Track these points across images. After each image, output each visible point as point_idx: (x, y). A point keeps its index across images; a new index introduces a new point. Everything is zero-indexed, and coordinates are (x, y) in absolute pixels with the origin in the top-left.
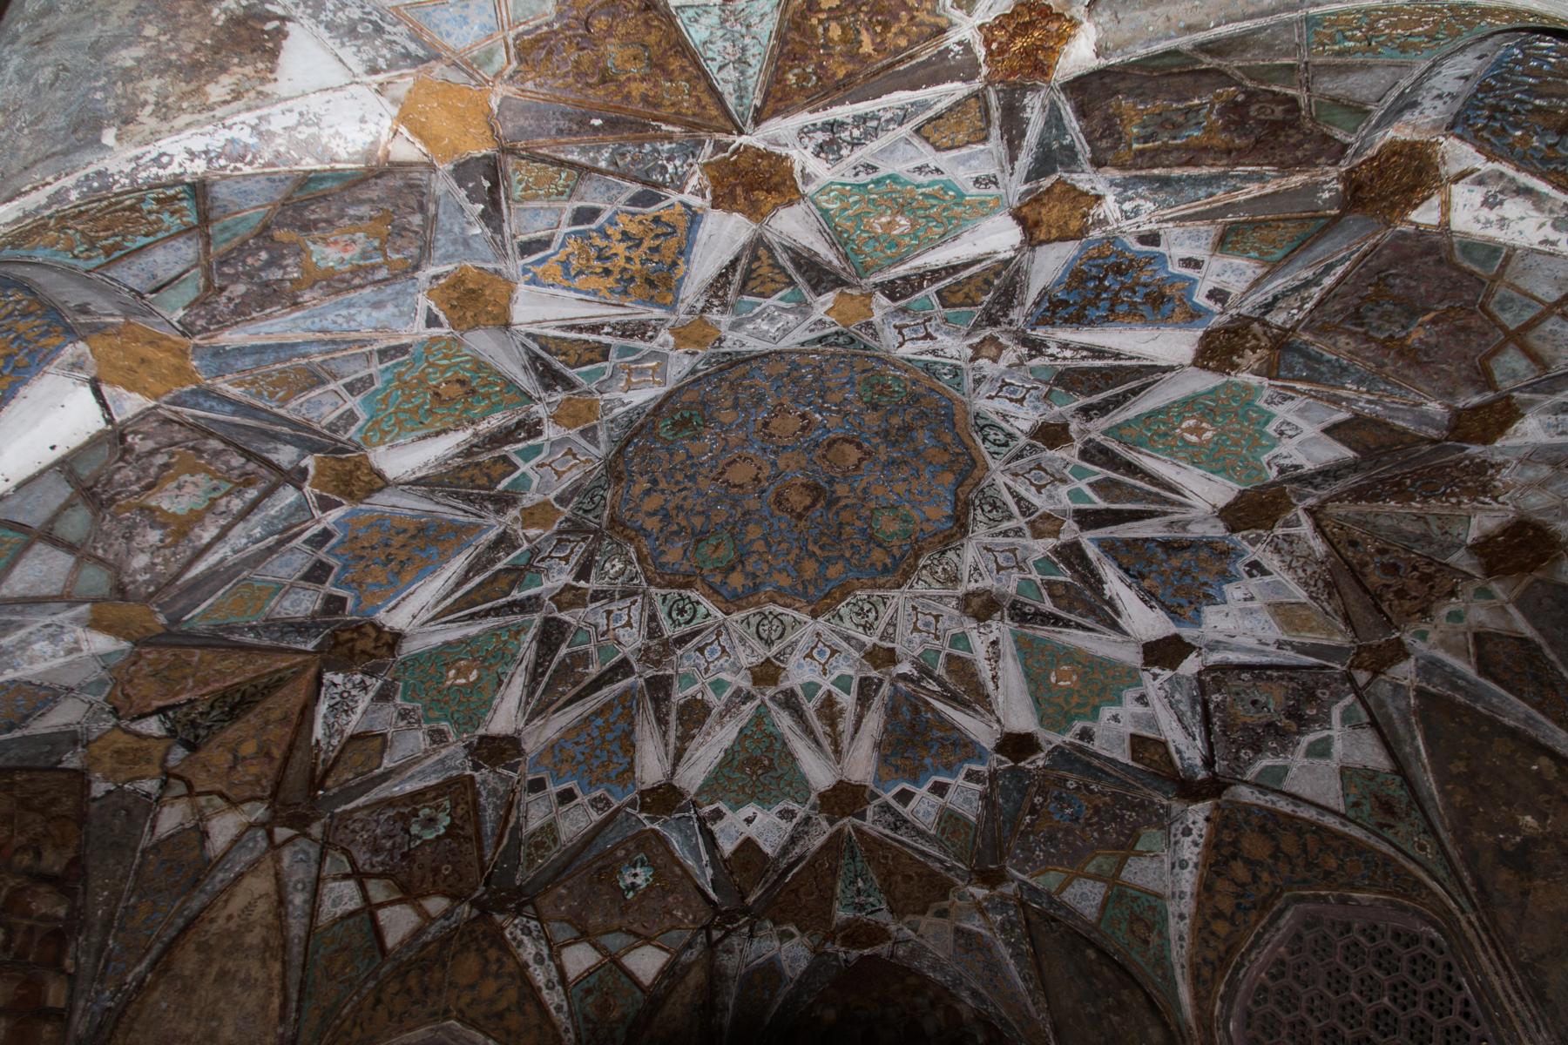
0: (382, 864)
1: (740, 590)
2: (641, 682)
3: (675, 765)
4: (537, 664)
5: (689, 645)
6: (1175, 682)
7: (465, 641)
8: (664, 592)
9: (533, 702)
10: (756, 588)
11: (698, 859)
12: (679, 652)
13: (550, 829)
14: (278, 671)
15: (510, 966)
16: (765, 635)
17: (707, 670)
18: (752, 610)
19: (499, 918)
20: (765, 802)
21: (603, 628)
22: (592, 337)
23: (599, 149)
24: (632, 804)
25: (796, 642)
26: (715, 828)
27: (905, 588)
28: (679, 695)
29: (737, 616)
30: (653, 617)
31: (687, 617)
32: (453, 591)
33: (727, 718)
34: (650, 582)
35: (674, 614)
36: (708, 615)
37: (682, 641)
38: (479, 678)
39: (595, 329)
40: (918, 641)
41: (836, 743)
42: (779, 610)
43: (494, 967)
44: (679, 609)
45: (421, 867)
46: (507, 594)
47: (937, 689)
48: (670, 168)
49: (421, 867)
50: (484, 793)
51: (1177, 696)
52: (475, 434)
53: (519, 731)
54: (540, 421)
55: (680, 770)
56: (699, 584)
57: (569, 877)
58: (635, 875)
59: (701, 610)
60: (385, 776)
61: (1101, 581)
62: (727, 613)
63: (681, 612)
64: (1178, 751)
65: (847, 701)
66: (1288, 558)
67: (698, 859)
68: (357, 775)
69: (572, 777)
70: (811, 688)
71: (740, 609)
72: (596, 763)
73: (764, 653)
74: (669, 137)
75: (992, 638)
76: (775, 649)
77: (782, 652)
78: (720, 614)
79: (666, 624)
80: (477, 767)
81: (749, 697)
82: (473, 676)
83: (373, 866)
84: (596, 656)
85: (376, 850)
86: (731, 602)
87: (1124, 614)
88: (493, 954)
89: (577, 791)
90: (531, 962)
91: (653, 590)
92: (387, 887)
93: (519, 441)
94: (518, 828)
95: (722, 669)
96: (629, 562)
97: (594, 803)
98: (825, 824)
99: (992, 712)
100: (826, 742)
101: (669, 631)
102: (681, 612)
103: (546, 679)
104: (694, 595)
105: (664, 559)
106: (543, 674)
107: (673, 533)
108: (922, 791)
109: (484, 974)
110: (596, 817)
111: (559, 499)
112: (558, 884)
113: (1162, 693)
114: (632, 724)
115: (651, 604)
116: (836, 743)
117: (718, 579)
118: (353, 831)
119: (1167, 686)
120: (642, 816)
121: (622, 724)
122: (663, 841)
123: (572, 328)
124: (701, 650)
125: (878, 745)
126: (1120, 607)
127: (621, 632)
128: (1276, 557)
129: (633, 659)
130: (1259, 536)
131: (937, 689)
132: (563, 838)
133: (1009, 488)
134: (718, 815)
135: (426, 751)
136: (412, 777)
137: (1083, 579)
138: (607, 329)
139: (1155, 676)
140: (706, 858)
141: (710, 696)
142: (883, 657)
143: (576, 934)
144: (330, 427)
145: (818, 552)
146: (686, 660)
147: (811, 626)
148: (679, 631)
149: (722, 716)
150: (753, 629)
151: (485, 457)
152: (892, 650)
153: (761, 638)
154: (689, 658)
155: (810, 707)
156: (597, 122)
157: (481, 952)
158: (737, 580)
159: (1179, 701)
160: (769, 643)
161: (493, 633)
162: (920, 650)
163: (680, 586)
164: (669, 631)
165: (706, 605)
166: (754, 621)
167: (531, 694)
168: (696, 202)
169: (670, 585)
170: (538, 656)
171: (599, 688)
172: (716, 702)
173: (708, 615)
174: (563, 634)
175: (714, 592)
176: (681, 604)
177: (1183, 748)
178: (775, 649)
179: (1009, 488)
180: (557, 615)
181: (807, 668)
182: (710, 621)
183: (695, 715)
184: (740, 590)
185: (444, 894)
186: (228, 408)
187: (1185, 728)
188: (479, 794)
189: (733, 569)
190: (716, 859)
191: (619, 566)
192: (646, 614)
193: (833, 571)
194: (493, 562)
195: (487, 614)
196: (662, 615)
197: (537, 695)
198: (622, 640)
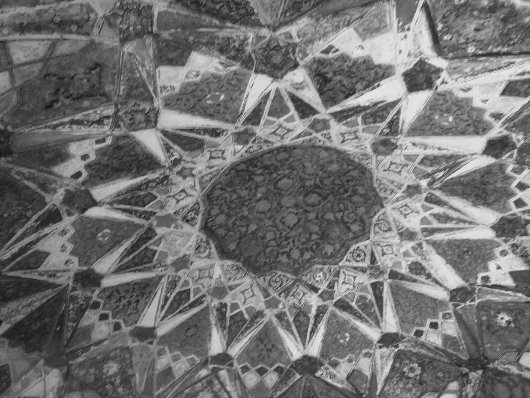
0: (417, 391)
1: (360, 228)
2: (389, 281)
3: (441, 285)
4: (355, 314)
5: (378, 259)
6: (452, 71)
7: (327, 335)
8: (345, 259)
9: (371, 322)
10: (362, 221)
11: (510, 295)
12: (379, 264)
13: (447, 339)
14: (305, 386)
15: (517, 380)
16: (386, 229)
17: (396, 255)
18: (372, 227)
19: (491, 366)
20: (491, 257)
21: (351, 287)
22: (169, 303)
23: (68, 327)
24: (455, 306)
25: (395, 220)
26: (493, 282)
27: (373, 171)
28: (404, 270)
29: (372, 235)
30: (355, 268)
31: (362, 254)
32: (294, 336)
33: (428, 257)
34: (336, 264)
35: (358, 259)
36: (366, 246)
37: (373, 260)
38: (350, 334)
39: (166, 299)
40: (406, 174)
41: (465, 222)
42: (376, 217)
43: (511, 384)
44: (358, 255)
45: (431, 381)
46: (309, 319)
47: (442, 173)
48: (81, 303)
49: (431, 381)
50: (412, 349)
51: (468, 70)
52: (216, 325)
53: (381, 333)
54: (221, 303)
55: (445, 285)
56: (351, 243)
57: (482, 339)
58: (502, 318)
59: (362, 248)
60: (374, 376)
61: (359, 106)
62: (369, 238)
63: (359, 255)
64: (523, 74)
65: (437, 210)
66: (317, 36)
67: (510, 295)
68: (366, 383)
69: (425, 319)
70: (424, 221)
71: (369, 232)
72: (423, 309)
73: (395, 232)
74: (67, 307)
75: (410, 145)
76: (394, 228)
77: (397, 227)
78: (367, 242)
79: (361, 264)
80: (397, 346)
81: (420, 245)
82: (347, 335)
83: (415, 394)
84: (363, 294)
85: (410, 390)
86: (364, 234)
87: (385, 99)
88: (505, 379)
89: (434, 321)
90: (520, 373)
91: (341, 264)
92: (429, 395)
93: (226, 311)
94: (437, 348)
95: (398, 250)
96: (322, 269)
97: (444, 316)
98: (524, 238)
99: (464, 156)
100: (461, 225)
101: (365, 264)
102: (359, 255)
103: (363, 315)
104: (354, 247)
105: (329, 254)
106: (360, 315)
107: (317, 247)
108: (520, 194)
109: (510, 389)
110: (453, 320)
111: (265, 297)
112: (483, 345)
113: (462, 79)
114: (411, 291)
115: (348, 267)
116: (465, 222)
117: (351, 235)
118: (393, 393)
119: (456, 76)
120: (468, 303)
121: (409, 294)
122: (488, 302)
123: (163, 307)
124: (384, 254)
125: (475, 205)
126: (379, 100)
127: (357, 281)
128: (316, 43)
129: (374, 280)
130: (300, 51)
131: (442, 173)
132: (456, 335)
133: (292, 140)
134: (486, 279)
135: (372, 361)
136: (382, 368)
137: (360, 112)
138: (169, 295)
139: (443, 82)
140: (510, 292)
141: (411, 259)
142: (413, 190)
143: (517, 353)
144: (191, 365)
145: (349, 194)
146: (386, 262)
147: (388, 208)
148: (368, 257)
149: (425, 259)
150: (381, 232)
151: (228, 324)
152: (409, 187)
153: (386, 231)
154: (385, 260)
155: (436, 224)
156: (58, 329)
157: (500, 381)
158: (355, 228)
159: (472, 70)
160: (390, 229)
161: (328, 323)
162: (413, 175)
163: (346, 252)
164: (365, 264)
165: (361, 245)
166: (377, 229)
167: (367, 322)
168: (97, 292)
169: (343, 256)
170: (351, 313)
171: (382, 298)
172: (415, 258)
173: (366, 246)
174: (344, 302)
175: (357, 238)
176: (355, 254)
177: (520, 71)
178: (394, 228)
179: (292, 140)
180: (334, 301)
181: (412, 219)
182: (369, 247)
183: (417, 268)
184: (360, 228)
185: (456, 379)
186: (170, 390)
187: (499, 68)
188: (410, 351)
189: (348, 228)
190: (515, 290)
191: (321, 274)
192: (352, 270)
193: (361, 190)
194: (287, 321)
195: (315, 325)
196: (356, 264)
197: (368, 319)
198: (361, 282)
